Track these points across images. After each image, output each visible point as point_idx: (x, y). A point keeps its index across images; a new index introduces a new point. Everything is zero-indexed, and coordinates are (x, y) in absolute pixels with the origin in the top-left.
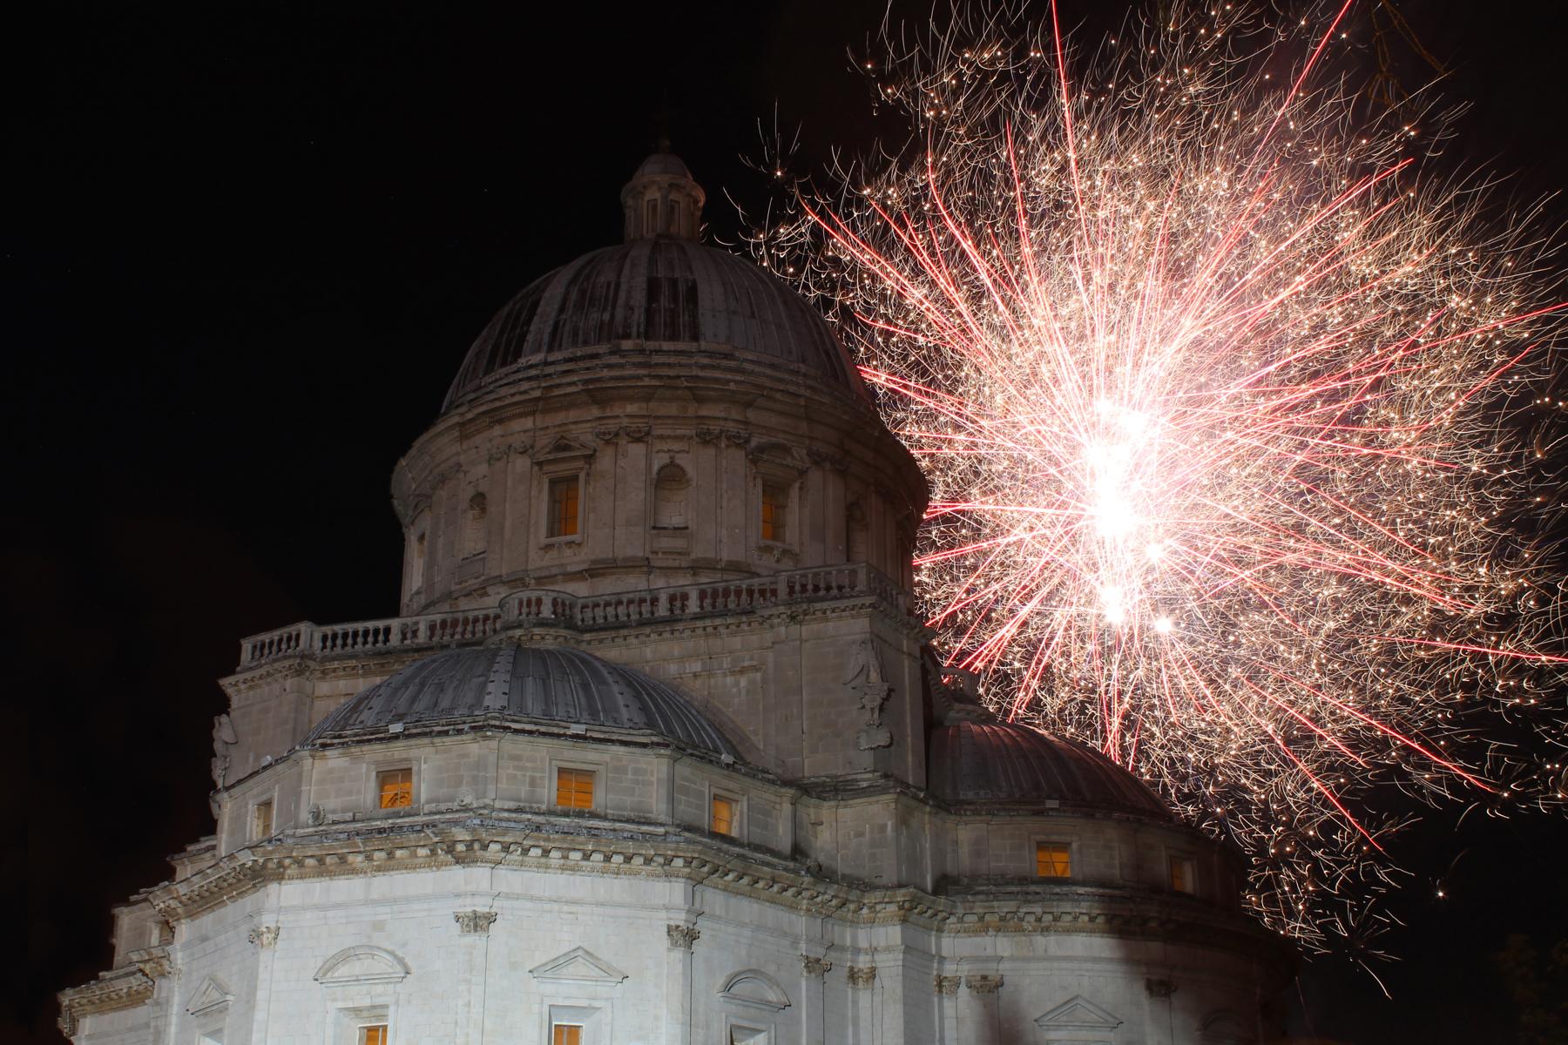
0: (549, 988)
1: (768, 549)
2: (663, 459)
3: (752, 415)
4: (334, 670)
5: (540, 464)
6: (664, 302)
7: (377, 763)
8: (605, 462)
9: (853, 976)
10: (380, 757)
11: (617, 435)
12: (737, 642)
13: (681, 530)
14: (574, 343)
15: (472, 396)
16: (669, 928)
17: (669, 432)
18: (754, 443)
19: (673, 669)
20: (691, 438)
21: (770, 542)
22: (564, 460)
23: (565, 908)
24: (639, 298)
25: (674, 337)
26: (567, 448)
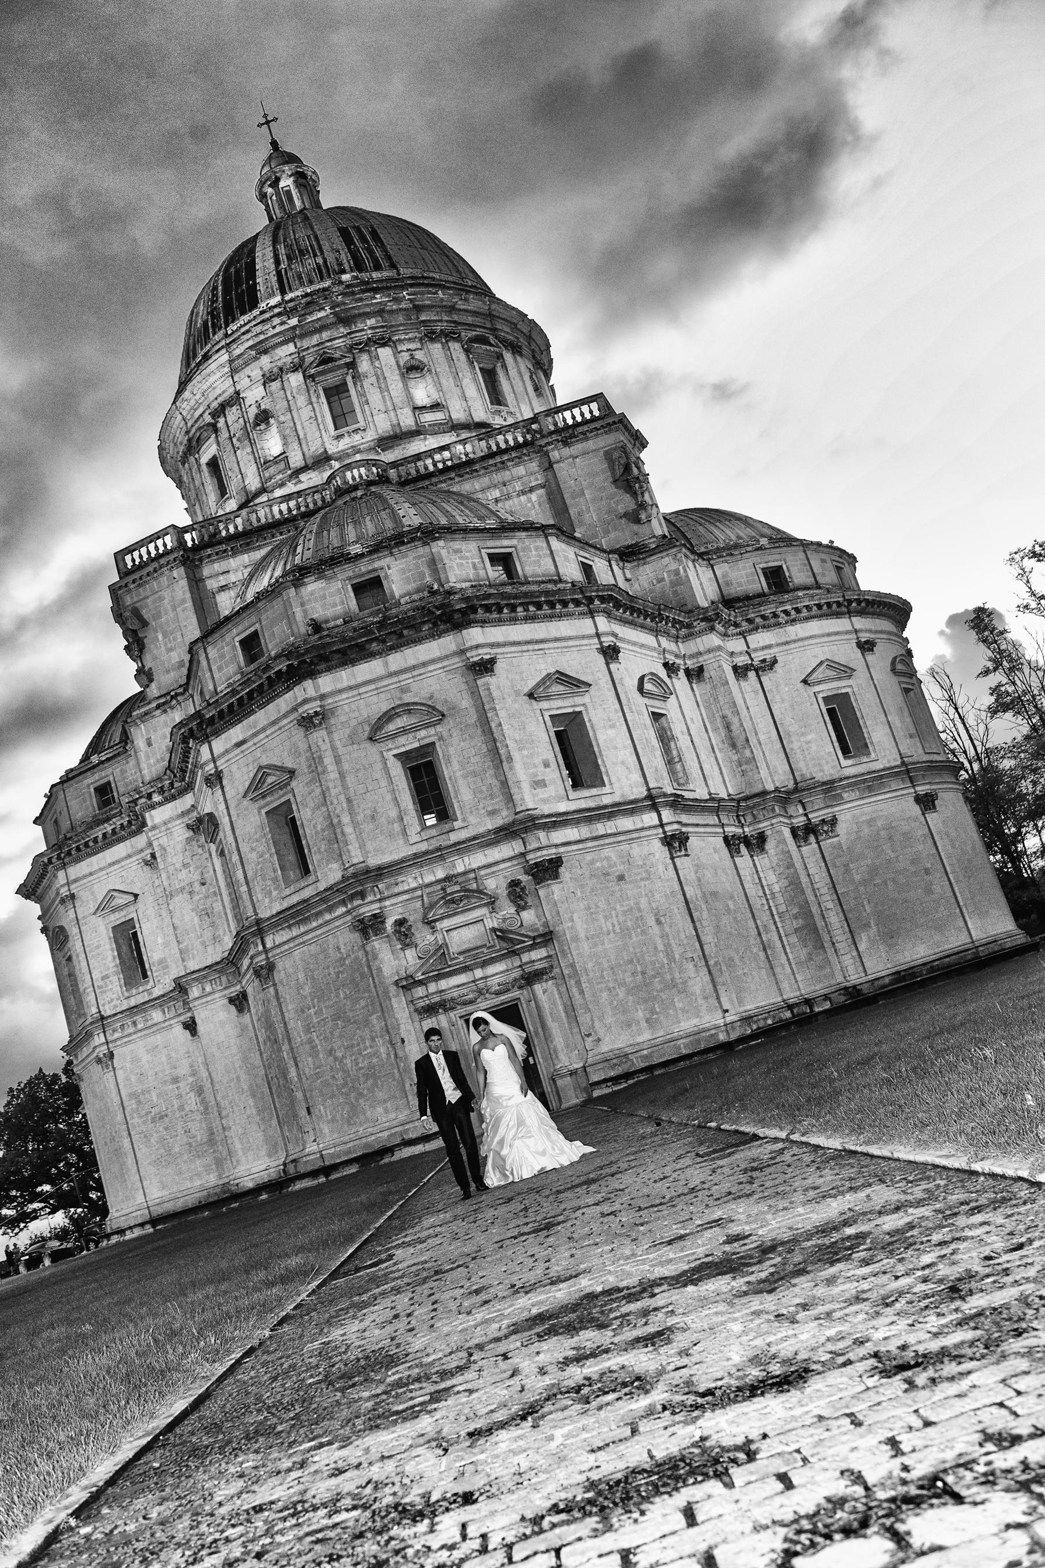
0: (544, 705)
2: (406, 356)
4: (209, 556)
5: (312, 377)
7: (350, 578)
8: (364, 364)
10: (351, 574)
12: (521, 470)
13: (436, 406)
14: (302, 284)
15: (223, 343)
18: (467, 335)
22: (331, 370)
23: (536, 647)
24: (339, 242)
25: (378, 267)
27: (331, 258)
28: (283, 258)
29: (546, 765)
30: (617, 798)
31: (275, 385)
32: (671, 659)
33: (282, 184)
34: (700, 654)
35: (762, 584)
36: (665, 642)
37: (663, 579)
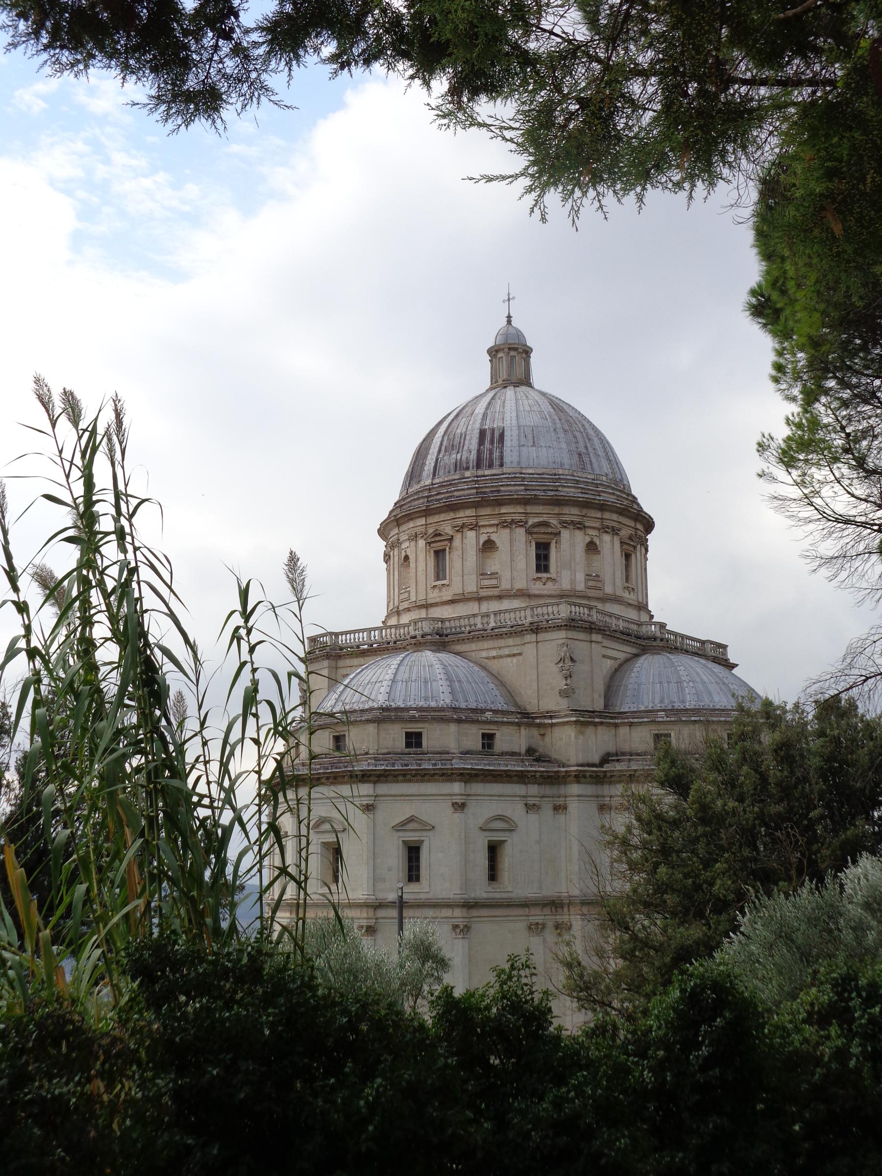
0: (401, 834)
1: (539, 579)
2: (483, 538)
3: (530, 509)
5: (430, 543)
6: (487, 445)
8: (457, 542)
9: (556, 808)
11: (462, 527)
13: (494, 575)
16: (453, 804)
17: (487, 523)
18: (530, 522)
19: (484, 654)
20: (497, 525)
21: (539, 575)
25: (491, 466)
26: (440, 535)
27: (464, 458)
28: (443, 448)
29: (389, 869)
30: (429, 896)
31: (413, 543)
32: (531, 801)
33: (500, 355)
34: (566, 797)
36: (534, 789)
37: (562, 739)
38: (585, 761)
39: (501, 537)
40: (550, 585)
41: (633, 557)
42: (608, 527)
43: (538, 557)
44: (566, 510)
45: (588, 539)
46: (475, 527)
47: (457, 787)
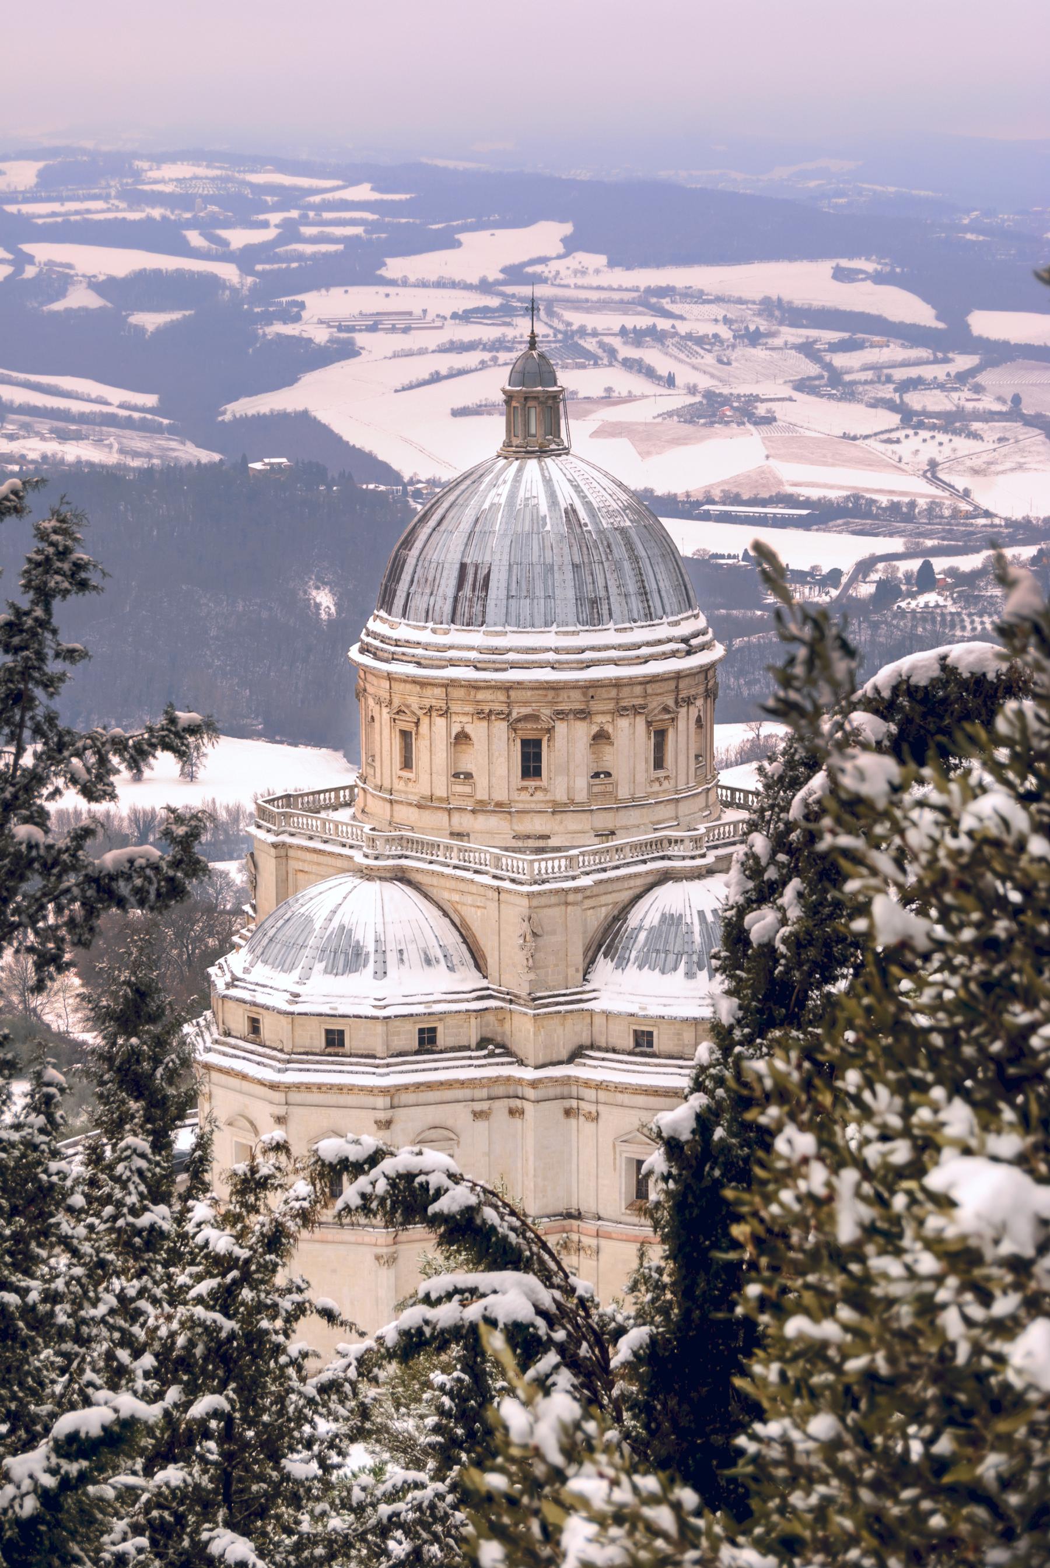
1: (524, 789)
2: (456, 729)
3: (512, 693)
6: (467, 590)
9: (512, 1112)
18: (514, 715)
19: (446, 895)
21: (526, 783)
32: (478, 1106)
35: (629, 1043)
38: (548, 1060)
39: (477, 730)
40: (539, 796)
41: (671, 735)
42: (625, 709)
43: (525, 757)
44: (564, 695)
45: (595, 729)
46: (446, 713)
47: (381, 1101)
